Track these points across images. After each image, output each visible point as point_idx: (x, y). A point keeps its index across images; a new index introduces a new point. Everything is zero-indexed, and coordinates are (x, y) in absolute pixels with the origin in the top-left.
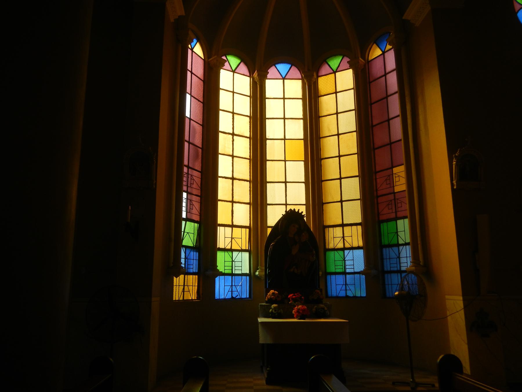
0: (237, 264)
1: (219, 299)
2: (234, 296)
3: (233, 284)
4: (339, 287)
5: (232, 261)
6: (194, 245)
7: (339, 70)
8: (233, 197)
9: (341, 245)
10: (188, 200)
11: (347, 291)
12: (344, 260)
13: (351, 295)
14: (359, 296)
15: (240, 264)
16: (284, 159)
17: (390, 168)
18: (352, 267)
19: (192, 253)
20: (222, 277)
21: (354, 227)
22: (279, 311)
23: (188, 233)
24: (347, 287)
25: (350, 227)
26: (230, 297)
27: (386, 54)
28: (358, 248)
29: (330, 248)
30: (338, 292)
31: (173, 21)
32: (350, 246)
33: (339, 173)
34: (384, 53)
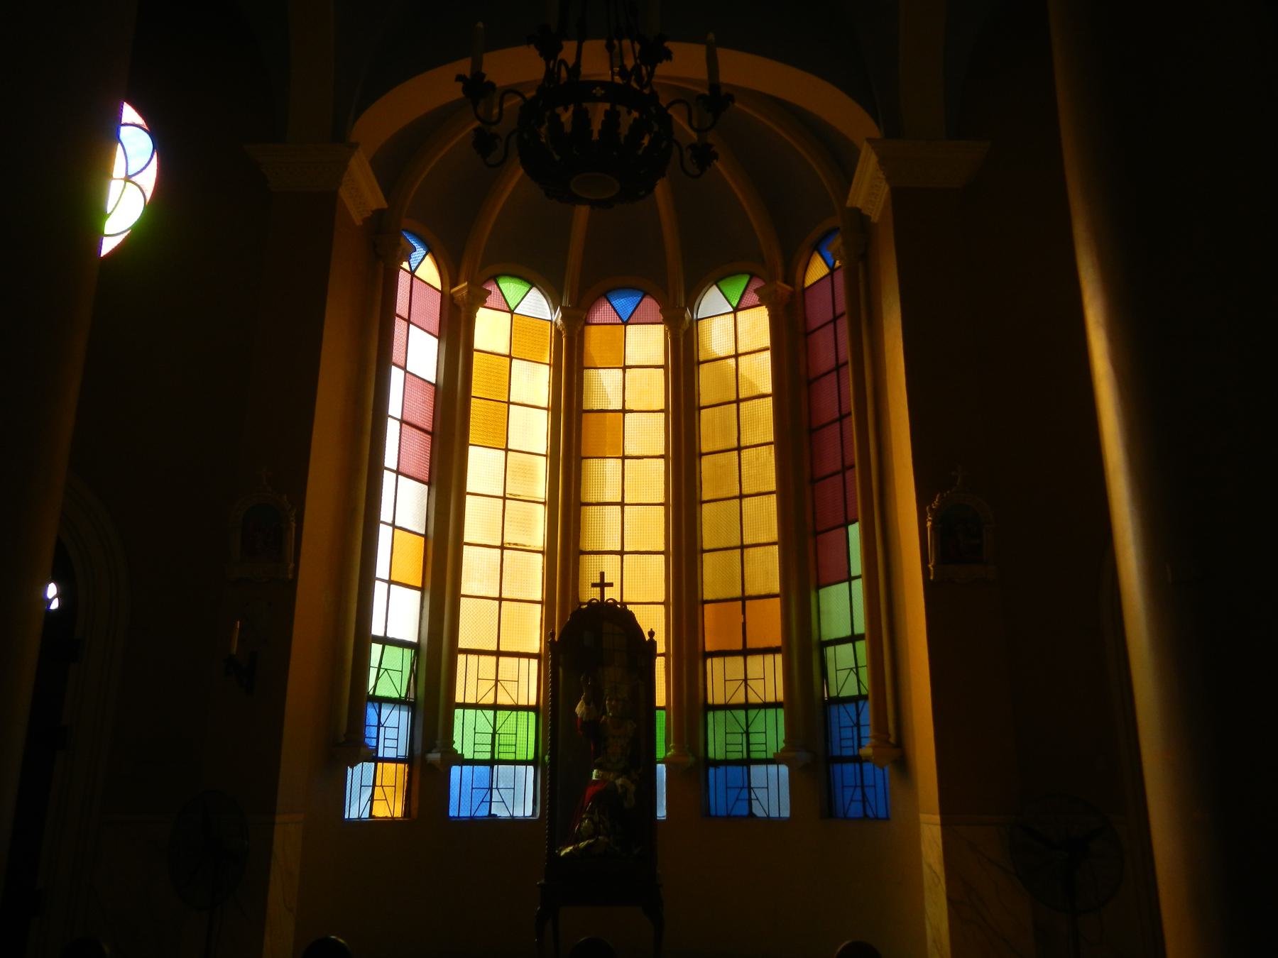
3: (494, 786)
6: (400, 696)
7: (744, 306)
12: (747, 733)
15: (511, 739)
17: (840, 526)
18: (763, 747)
19: (396, 712)
23: (386, 670)
25: (759, 658)
27: (835, 273)
28: (776, 705)
30: (730, 807)
31: (361, 223)
32: (759, 701)
34: (832, 270)
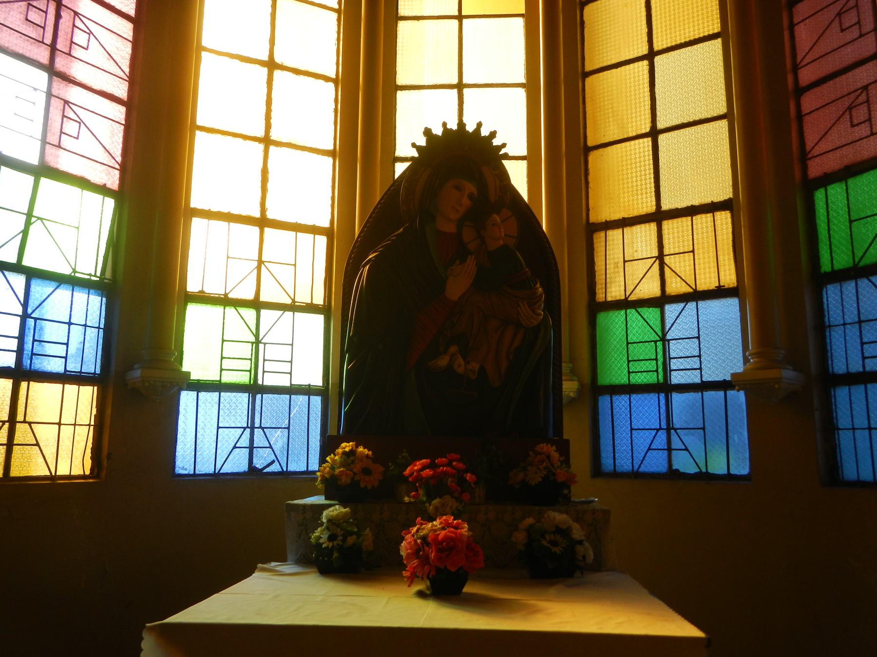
0: (271, 352)
1: (195, 475)
2: (259, 463)
3: (257, 425)
4: (642, 440)
5: (257, 342)
6: (74, 271)
8: (268, 126)
9: (650, 288)
10: (54, 101)
11: (674, 452)
12: (664, 339)
13: (692, 469)
14: (723, 471)
16: (456, 13)
20: (208, 398)
21: (703, 221)
22: (351, 540)
23: (39, 218)
24: (674, 437)
25: (686, 221)
26: (243, 467)
28: (720, 293)
29: (609, 299)
32: (686, 289)
33: (645, 39)
